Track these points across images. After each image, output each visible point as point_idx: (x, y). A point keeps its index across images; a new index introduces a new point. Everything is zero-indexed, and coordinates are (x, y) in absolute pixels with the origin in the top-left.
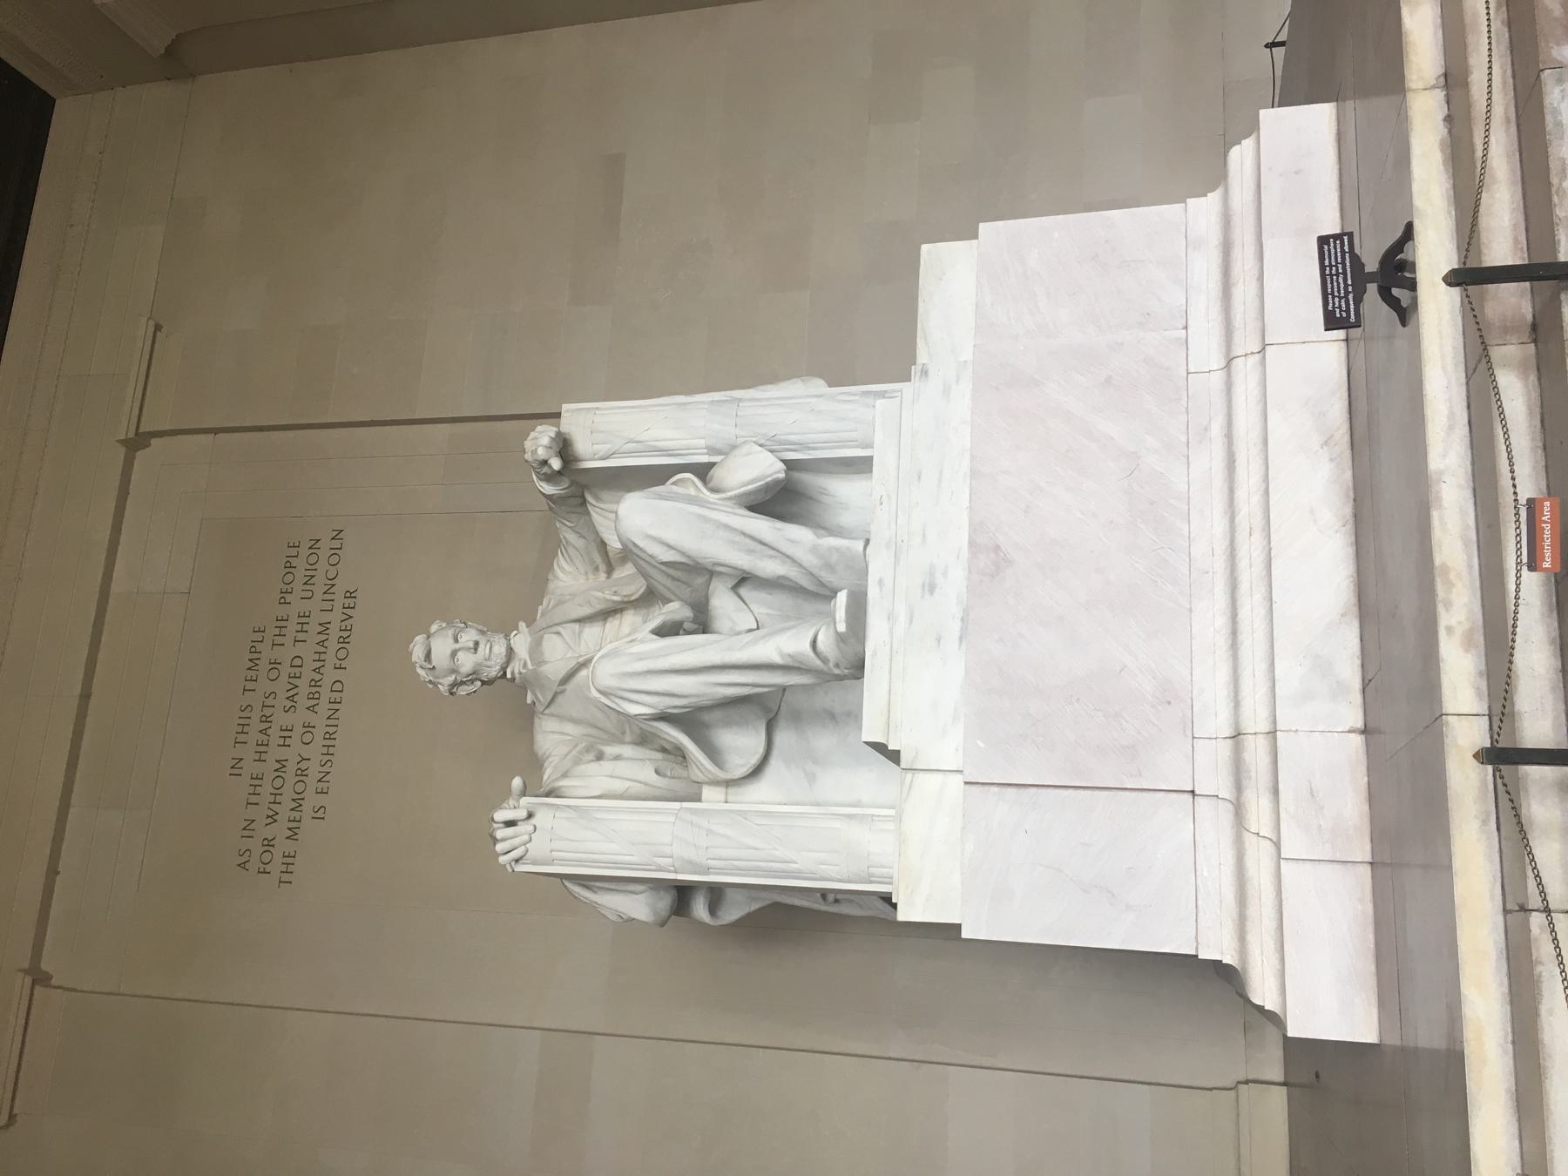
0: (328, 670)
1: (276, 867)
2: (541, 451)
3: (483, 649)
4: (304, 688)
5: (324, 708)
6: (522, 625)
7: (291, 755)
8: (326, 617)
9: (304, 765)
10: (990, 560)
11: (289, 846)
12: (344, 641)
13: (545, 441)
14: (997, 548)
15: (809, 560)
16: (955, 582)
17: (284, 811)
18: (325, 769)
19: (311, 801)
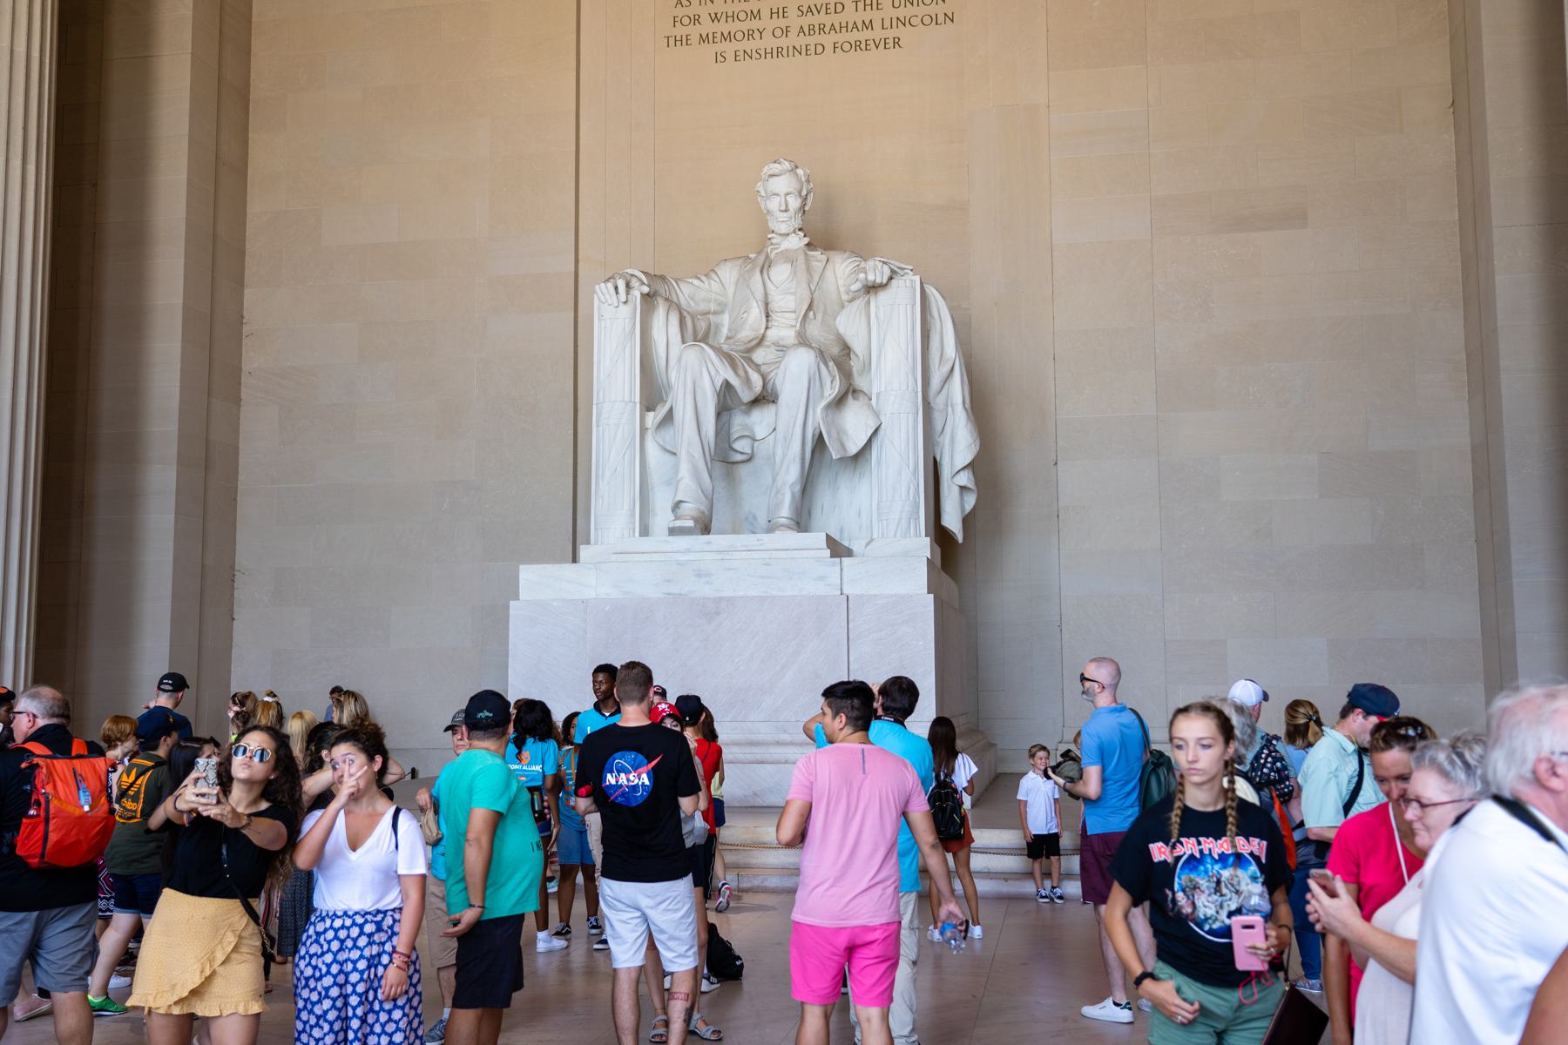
0: (834, 37)
1: (680, 31)
2: (862, 276)
3: (783, 216)
4: (816, 19)
5: (802, 41)
6: (806, 240)
7: (766, 23)
8: (877, 25)
9: (757, 35)
10: (711, 610)
11: (695, 39)
12: (857, 45)
13: (871, 277)
14: (718, 614)
15: (779, 483)
16: (703, 590)
17: (723, 27)
18: (755, 55)
19: (729, 48)
